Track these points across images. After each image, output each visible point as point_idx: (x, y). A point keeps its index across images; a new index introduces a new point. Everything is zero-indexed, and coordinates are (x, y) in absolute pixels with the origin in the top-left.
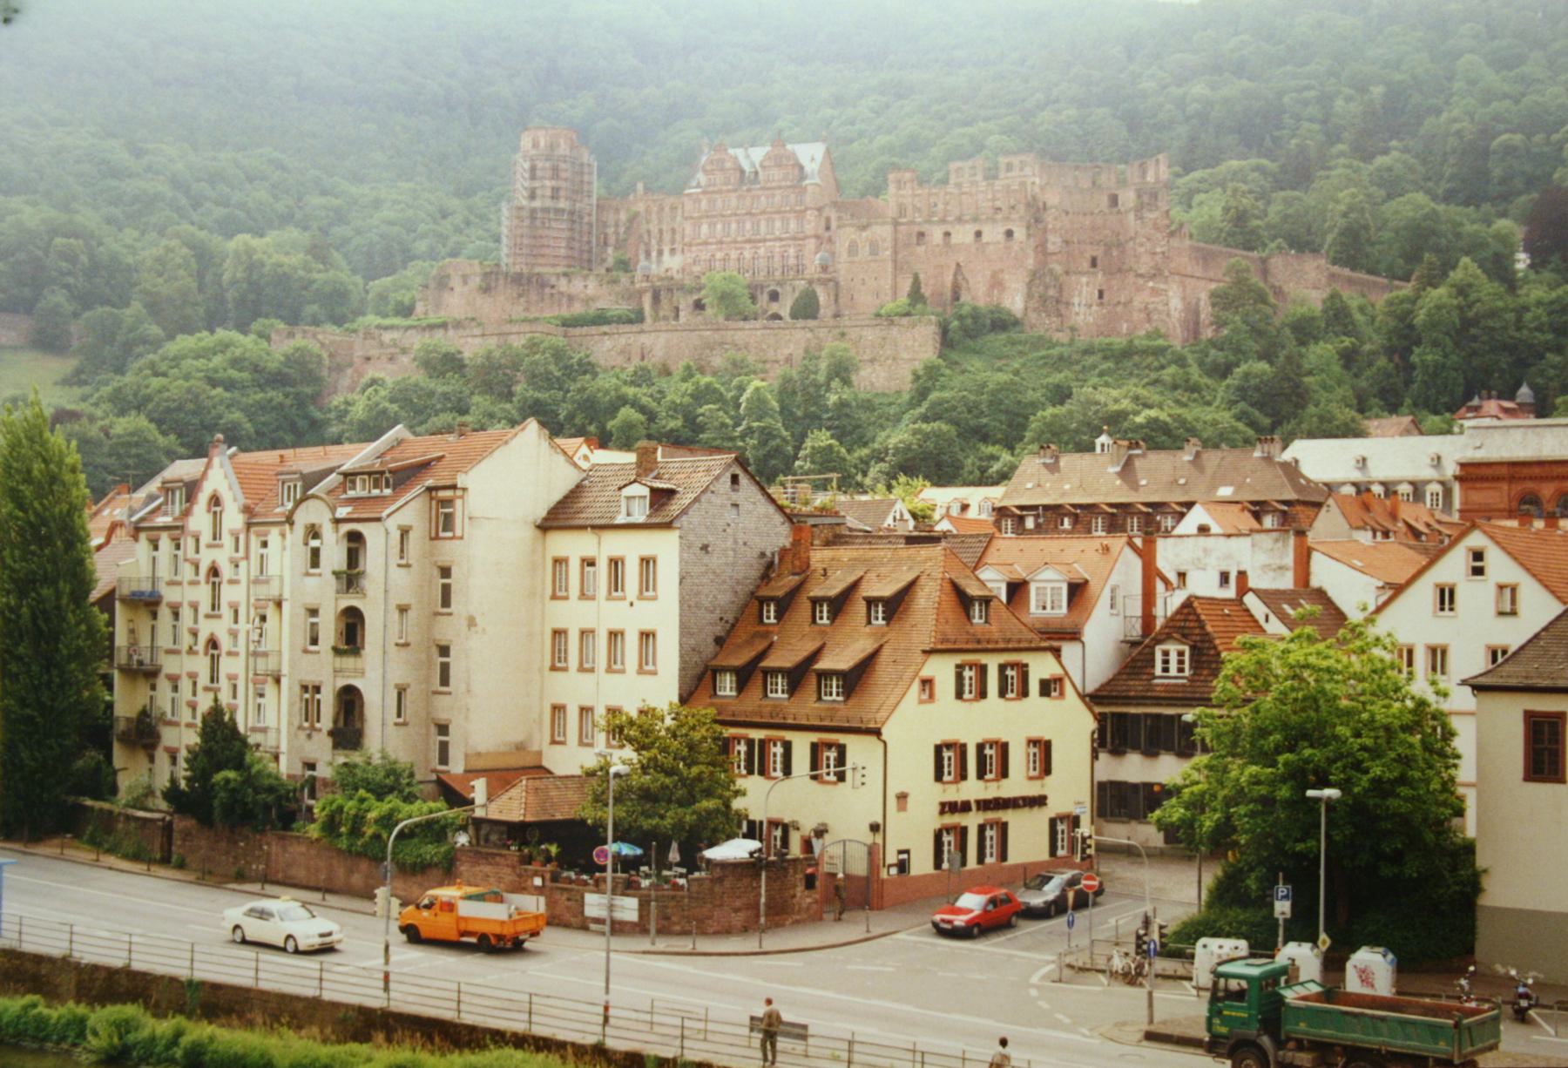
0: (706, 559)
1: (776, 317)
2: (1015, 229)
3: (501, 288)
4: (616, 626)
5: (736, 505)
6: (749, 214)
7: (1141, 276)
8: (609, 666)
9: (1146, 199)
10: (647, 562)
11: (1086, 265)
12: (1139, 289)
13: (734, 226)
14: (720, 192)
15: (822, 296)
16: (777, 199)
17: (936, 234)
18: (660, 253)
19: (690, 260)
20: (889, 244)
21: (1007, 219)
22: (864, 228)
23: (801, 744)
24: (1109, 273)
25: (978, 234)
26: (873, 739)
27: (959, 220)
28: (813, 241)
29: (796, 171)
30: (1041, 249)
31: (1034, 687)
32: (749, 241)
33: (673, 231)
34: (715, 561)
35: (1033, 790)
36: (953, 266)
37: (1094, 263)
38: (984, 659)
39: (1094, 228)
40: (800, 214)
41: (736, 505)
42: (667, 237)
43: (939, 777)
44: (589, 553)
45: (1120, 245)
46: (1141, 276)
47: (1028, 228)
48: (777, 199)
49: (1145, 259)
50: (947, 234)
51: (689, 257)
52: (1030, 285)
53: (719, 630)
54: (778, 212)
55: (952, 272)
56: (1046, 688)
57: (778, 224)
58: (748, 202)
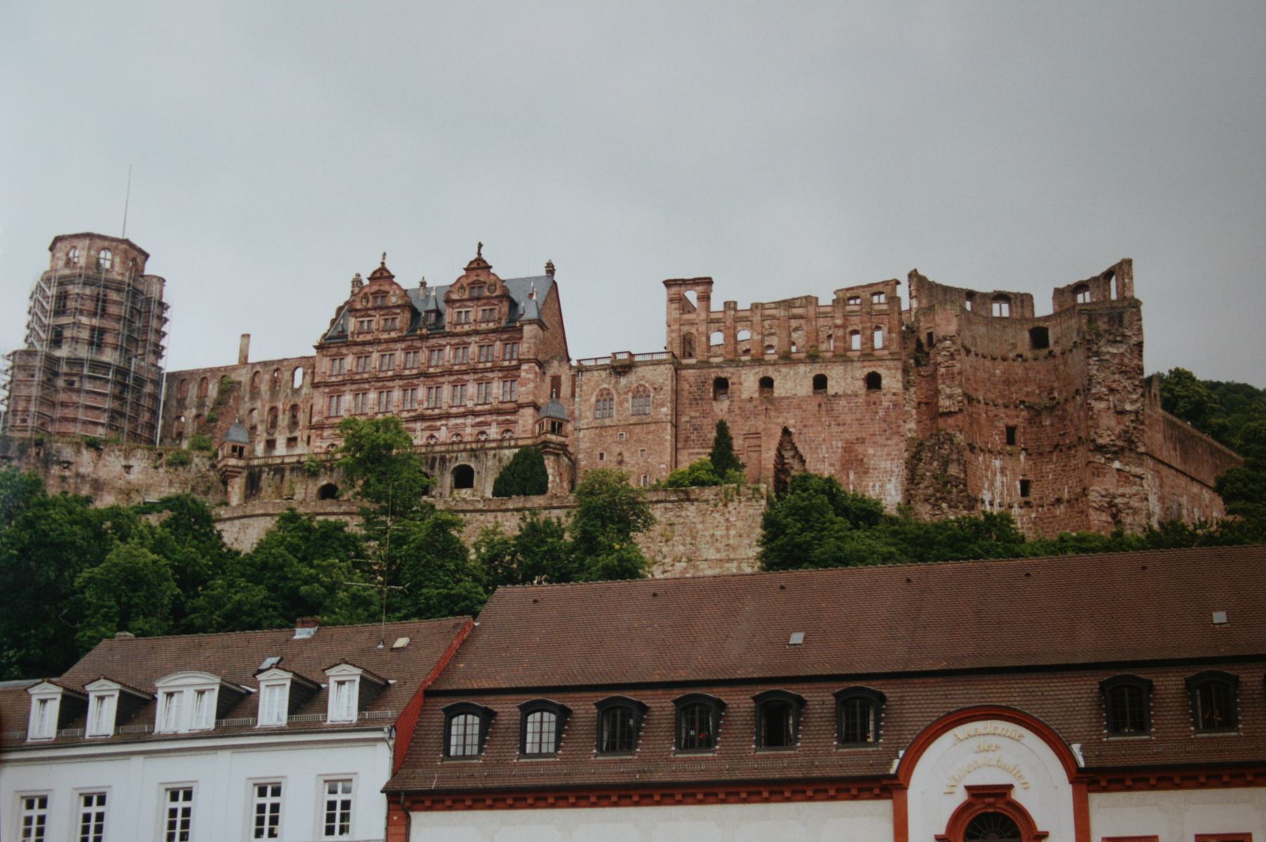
2: (882, 371)
7: (1100, 449)
9: (1102, 325)
11: (998, 439)
12: (1098, 472)
14: (377, 342)
16: (473, 349)
17: (748, 382)
20: (667, 395)
25: (820, 383)
27: (786, 358)
28: (530, 411)
29: (505, 308)
30: (929, 408)
32: (421, 418)
36: (778, 432)
37: (1010, 434)
39: (1007, 382)
40: (510, 374)
42: (284, 420)
46: (1100, 449)
47: (905, 371)
48: (473, 349)
49: (1113, 423)
50: (766, 383)
54: (475, 371)
55: (774, 444)
57: (471, 389)
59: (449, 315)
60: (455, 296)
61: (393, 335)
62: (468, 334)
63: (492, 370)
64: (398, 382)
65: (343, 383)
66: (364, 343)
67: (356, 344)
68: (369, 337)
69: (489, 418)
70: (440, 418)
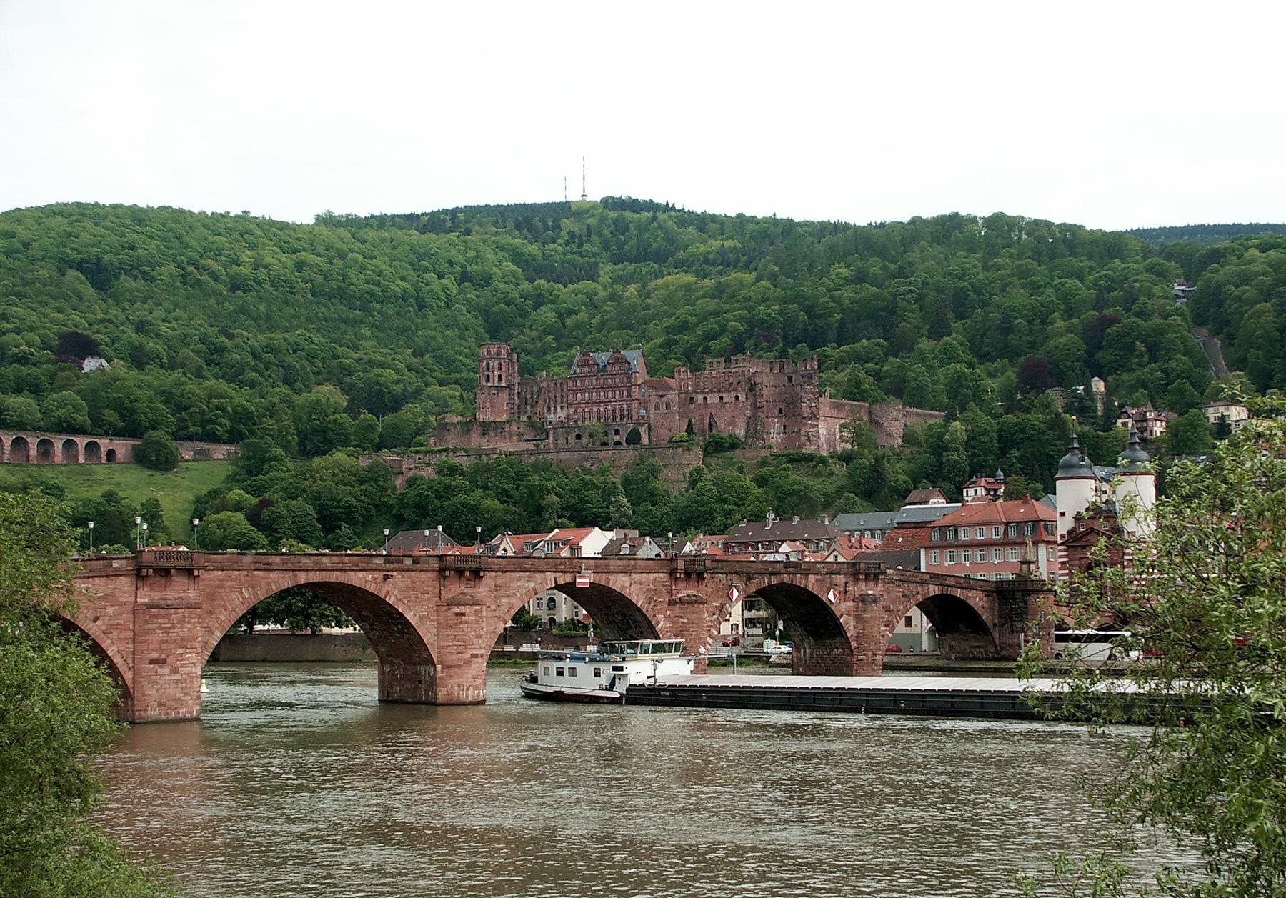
12: (804, 425)
15: (643, 432)
17: (700, 399)
18: (556, 409)
21: (736, 390)
22: (662, 396)
24: (788, 417)
25: (721, 398)
27: (711, 392)
42: (559, 400)
45: (794, 403)
51: (572, 411)
52: (748, 424)
59: (609, 368)
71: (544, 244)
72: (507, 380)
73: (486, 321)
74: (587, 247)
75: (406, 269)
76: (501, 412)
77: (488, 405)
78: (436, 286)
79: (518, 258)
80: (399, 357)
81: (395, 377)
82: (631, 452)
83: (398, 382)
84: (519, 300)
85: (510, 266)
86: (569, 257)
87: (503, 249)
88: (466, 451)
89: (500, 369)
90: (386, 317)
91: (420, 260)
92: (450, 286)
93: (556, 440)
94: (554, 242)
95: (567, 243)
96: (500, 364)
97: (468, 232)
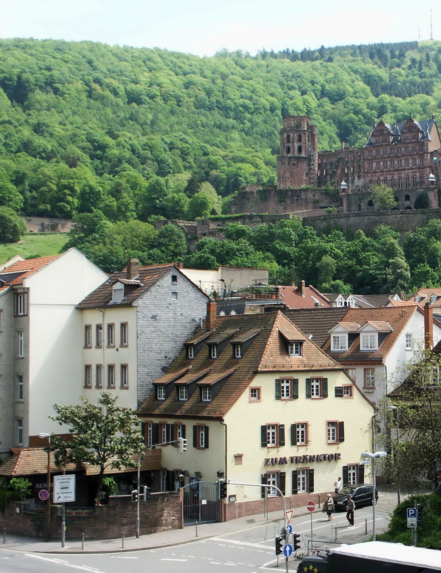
0: (155, 324)
1: (409, 208)
3: (272, 197)
4: (111, 363)
5: (175, 293)
6: (396, 156)
8: (122, 385)
10: (124, 326)
13: (389, 163)
14: (381, 146)
16: (410, 148)
19: (367, 181)
23: (189, 425)
26: (218, 423)
31: (331, 392)
33: (359, 166)
34: (161, 325)
35: (332, 450)
38: (295, 376)
40: (422, 156)
41: (175, 293)
43: (264, 444)
44: (100, 322)
48: (410, 148)
51: (368, 179)
53: (164, 363)
54: (411, 155)
56: (339, 392)
57: (411, 161)
58: (396, 151)
60: (404, 131)
61: (386, 143)
62: (408, 143)
63: (416, 155)
64: (389, 159)
65: (372, 159)
66: (378, 146)
67: (375, 146)
68: (379, 144)
69: (416, 170)
70: (402, 170)
71: (391, 68)
72: (307, 151)
73: (339, 128)
74: (425, 70)
75: (275, 88)
76: (300, 182)
77: (288, 175)
78: (299, 100)
79: (369, 80)
80: (260, 154)
81: (253, 170)
82: (419, 216)
83: (255, 174)
84: (366, 110)
85: (360, 85)
86: (411, 77)
87: (356, 72)
88: (261, 217)
89: (300, 140)
90: (254, 124)
91: (287, 82)
92: (310, 100)
93: (349, 206)
94: (399, 66)
95: (410, 67)
96: (300, 136)
97: (330, 60)
